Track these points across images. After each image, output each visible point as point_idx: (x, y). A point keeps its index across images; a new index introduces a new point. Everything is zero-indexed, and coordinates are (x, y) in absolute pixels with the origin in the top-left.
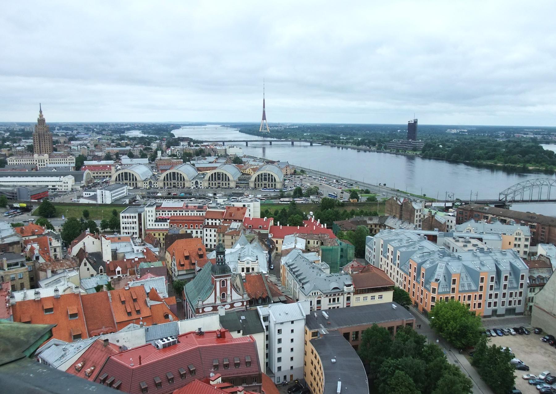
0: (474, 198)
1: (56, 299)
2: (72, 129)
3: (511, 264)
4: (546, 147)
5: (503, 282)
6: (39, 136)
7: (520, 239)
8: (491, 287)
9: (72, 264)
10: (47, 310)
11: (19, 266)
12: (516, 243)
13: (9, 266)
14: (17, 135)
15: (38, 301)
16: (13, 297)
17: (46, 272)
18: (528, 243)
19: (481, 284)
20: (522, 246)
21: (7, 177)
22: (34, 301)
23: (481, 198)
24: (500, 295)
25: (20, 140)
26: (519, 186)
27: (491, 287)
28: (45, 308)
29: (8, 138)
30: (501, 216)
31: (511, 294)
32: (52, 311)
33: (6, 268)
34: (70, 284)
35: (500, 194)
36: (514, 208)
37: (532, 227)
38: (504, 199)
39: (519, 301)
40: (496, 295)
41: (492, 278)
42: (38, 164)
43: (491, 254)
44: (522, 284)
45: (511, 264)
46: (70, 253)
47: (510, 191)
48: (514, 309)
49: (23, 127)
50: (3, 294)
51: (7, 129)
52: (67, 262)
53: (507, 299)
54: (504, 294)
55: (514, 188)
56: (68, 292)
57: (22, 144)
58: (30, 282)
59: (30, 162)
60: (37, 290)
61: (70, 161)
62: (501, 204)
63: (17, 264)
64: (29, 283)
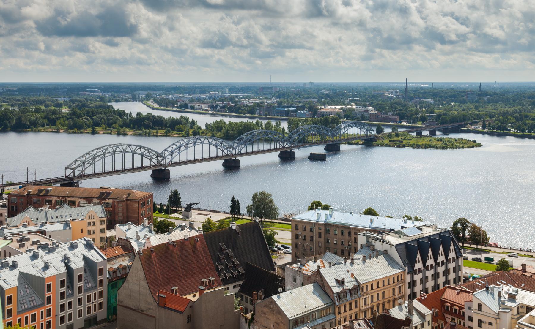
0: (32, 178)
3: (85, 259)
4: (117, 106)
5: (77, 284)
7: (94, 224)
8: (62, 294)
12: (89, 228)
18: (104, 226)
19: (48, 294)
20: (98, 232)
23: (41, 177)
24: (75, 303)
26: (88, 156)
27: (62, 294)
30: (69, 197)
31: (89, 299)
35: (66, 168)
36: (85, 184)
37: (107, 205)
38: (72, 174)
39: (101, 304)
40: (70, 304)
41: (62, 282)
43: (57, 250)
44: (101, 281)
45: (85, 259)
47: (78, 163)
48: (95, 317)
53: (86, 304)
54: (80, 300)
55: (83, 159)
62: (69, 182)
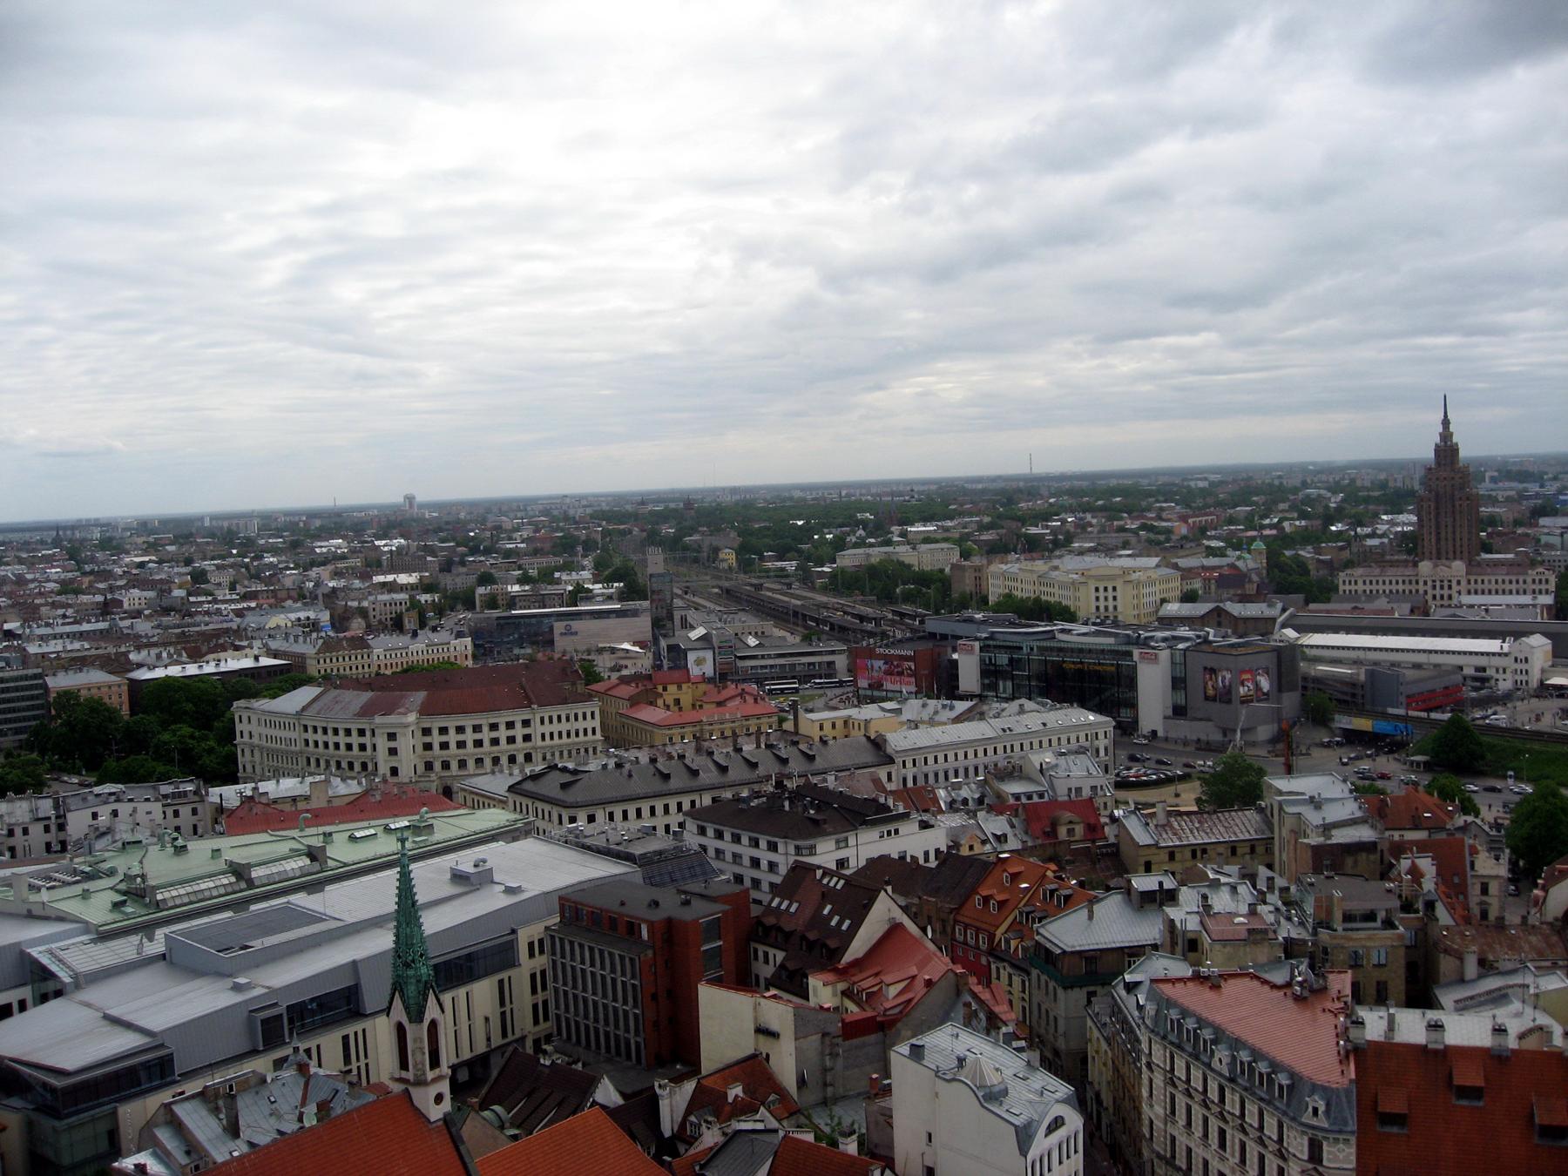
1: (1494, 1060)
2: (1538, 478)
6: (1437, 502)
9: (1551, 946)
10: (1463, 1092)
11: (1378, 924)
13: (1348, 918)
14: (1367, 500)
15: (1436, 1052)
16: (1360, 1023)
17: (1461, 959)
21: (1336, 632)
22: (1422, 1050)
25: (1376, 515)
28: (1456, 1082)
29: (1339, 509)
32: (1479, 1098)
33: (1339, 926)
34: (1543, 1019)
42: (1430, 592)
46: (1539, 903)
49: (1382, 476)
50: (1329, 1005)
51: (1337, 483)
52: (1533, 939)
56: (1531, 1044)
57: (1382, 528)
58: (1407, 982)
59: (1407, 587)
60: (1432, 1015)
61: (1537, 587)
63: (1370, 916)
64: (1403, 987)
